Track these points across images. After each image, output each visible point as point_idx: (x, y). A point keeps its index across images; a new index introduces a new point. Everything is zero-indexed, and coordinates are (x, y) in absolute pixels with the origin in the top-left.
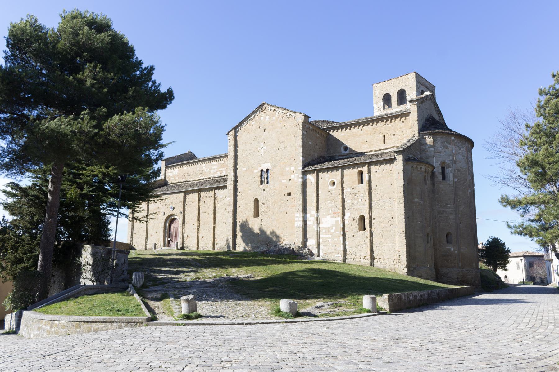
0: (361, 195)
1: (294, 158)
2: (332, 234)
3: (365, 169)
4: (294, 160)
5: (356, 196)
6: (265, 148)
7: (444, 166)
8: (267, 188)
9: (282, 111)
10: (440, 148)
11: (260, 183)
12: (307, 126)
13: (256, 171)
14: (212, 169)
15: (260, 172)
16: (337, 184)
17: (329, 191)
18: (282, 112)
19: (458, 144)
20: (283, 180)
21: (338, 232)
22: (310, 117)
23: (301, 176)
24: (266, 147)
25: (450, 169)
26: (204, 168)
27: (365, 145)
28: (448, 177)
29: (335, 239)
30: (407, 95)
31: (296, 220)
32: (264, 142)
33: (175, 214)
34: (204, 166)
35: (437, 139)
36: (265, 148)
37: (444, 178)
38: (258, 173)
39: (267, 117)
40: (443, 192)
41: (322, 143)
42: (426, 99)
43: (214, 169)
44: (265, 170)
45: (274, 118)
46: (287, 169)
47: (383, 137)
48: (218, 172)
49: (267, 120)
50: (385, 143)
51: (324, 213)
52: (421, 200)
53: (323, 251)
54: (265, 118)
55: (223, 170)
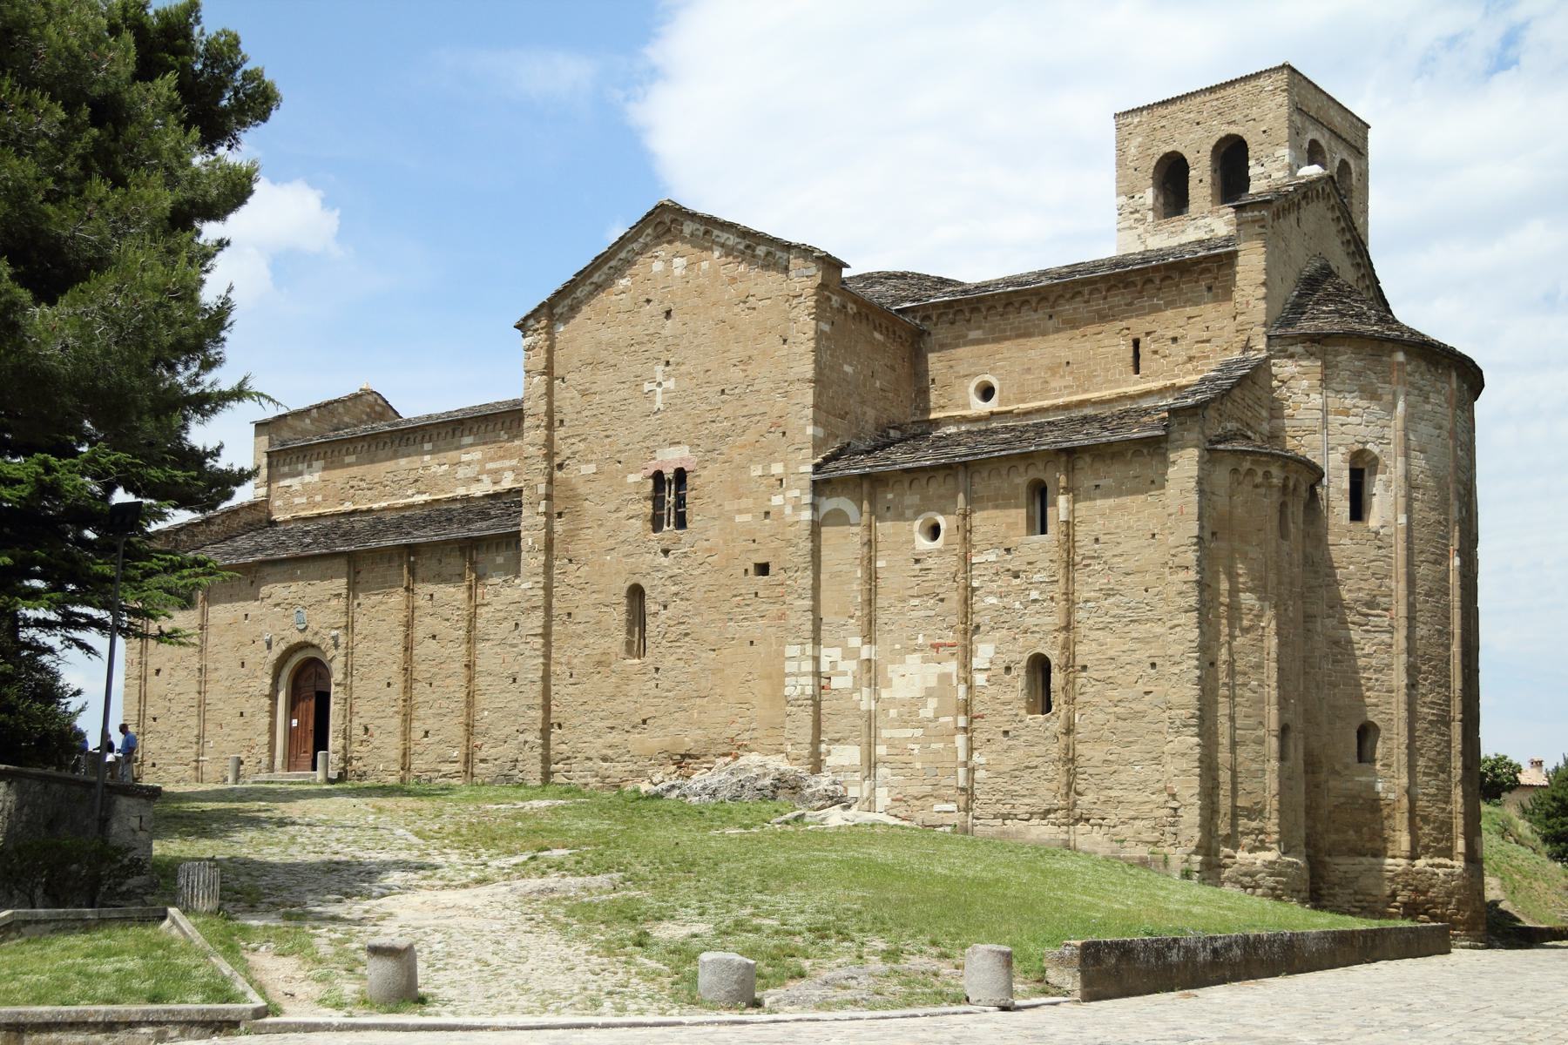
0: (1037, 577)
1: (781, 430)
4: (784, 433)
6: (670, 384)
7: (1360, 466)
8: (676, 546)
13: (632, 478)
15: (651, 481)
16: (948, 530)
20: (740, 512)
23: (807, 498)
24: (673, 379)
27: (1063, 377)
29: (934, 746)
30: (1251, 163)
32: (668, 363)
35: (1339, 359)
36: (670, 384)
37: (1358, 510)
41: (893, 368)
42: (1305, 196)
44: (669, 473)
45: (705, 265)
49: (677, 272)
50: (1137, 372)
55: (505, 469)
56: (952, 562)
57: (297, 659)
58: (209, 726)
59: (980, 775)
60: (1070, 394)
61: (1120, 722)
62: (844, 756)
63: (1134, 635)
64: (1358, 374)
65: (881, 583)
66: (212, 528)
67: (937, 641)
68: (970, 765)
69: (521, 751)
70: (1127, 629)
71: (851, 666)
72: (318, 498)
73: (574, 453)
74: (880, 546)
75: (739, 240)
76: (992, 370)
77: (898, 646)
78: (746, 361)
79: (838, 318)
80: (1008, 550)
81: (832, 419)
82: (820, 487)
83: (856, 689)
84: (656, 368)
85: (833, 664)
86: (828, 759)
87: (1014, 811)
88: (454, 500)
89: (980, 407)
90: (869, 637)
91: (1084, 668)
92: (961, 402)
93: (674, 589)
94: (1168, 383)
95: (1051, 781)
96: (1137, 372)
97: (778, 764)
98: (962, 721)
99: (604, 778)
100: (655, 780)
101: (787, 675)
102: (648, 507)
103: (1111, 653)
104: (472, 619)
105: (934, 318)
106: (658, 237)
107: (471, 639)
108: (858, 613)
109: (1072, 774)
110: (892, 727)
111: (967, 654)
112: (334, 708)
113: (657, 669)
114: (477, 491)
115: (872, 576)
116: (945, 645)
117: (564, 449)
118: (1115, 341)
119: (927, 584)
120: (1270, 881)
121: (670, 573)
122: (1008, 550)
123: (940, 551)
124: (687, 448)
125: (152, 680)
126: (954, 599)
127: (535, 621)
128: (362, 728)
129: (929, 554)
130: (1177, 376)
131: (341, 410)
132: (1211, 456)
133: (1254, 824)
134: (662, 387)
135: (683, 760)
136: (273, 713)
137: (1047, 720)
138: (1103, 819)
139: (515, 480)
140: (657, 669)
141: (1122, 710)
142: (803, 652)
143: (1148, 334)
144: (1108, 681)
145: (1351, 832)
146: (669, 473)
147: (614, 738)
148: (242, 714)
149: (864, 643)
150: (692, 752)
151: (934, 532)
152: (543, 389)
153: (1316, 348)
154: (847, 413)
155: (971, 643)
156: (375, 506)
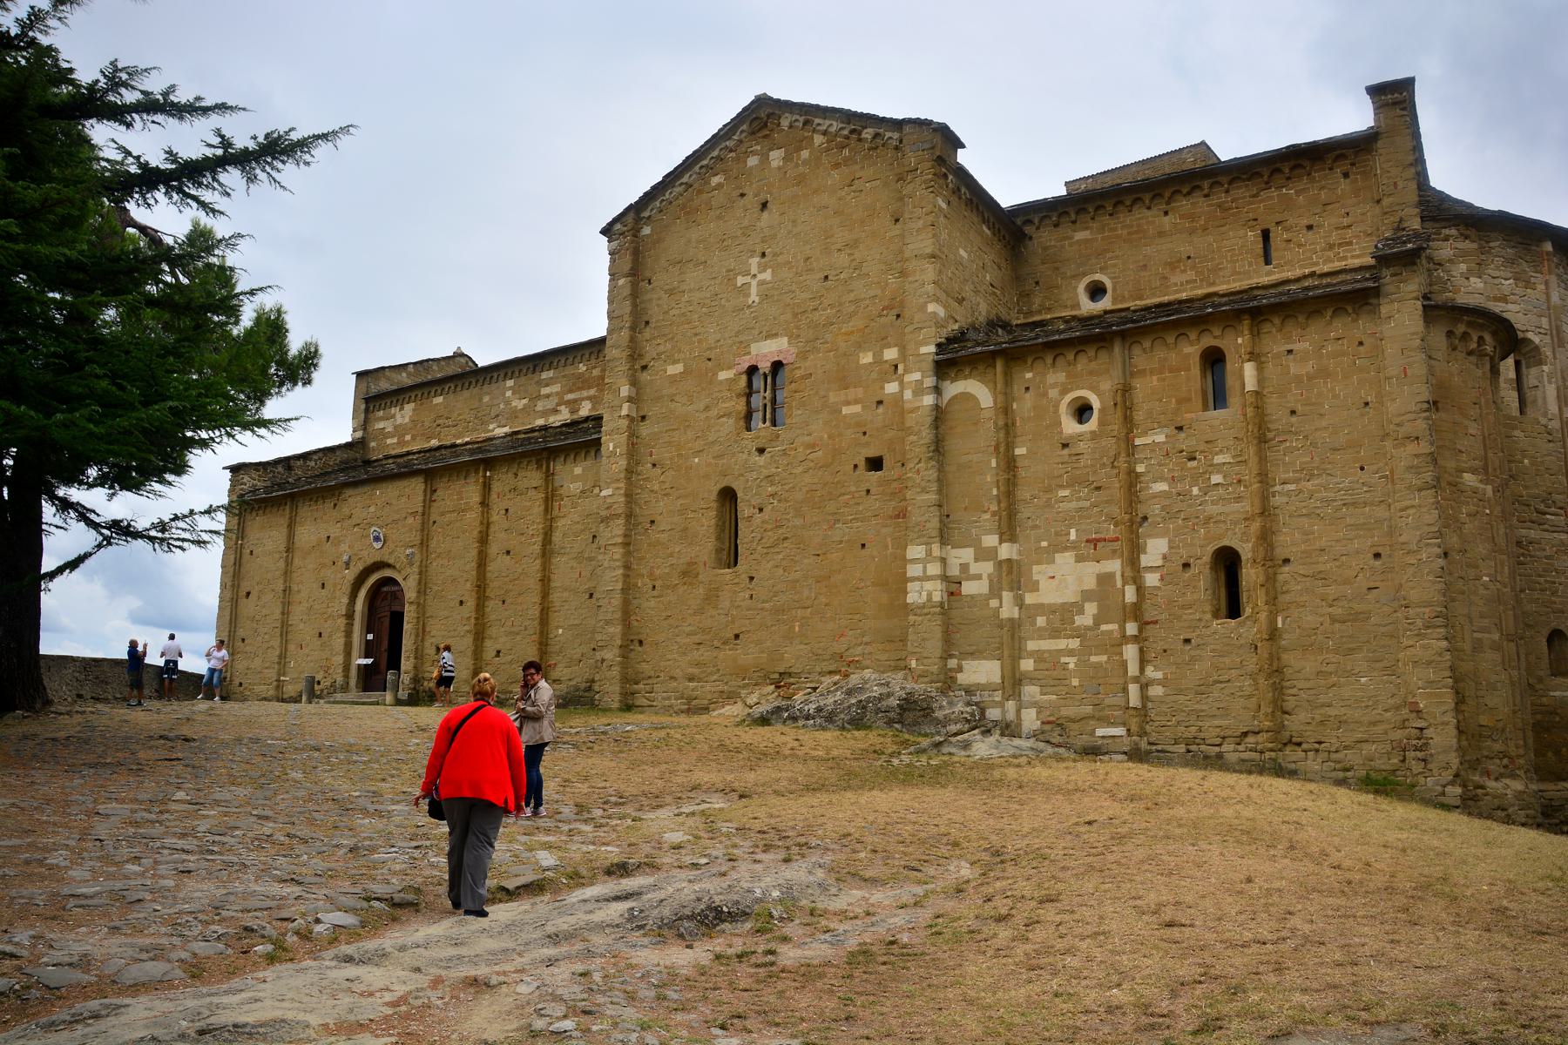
0: (1219, 459)
2: (1079, 633)
3: (1235, 343)
5: (1194, 463)
6: (767, 275)
8: (774, 444)
9: (841, 125)
10: (1503, 281)
11: (742, 423)
13: (723, 375)
14: (539, 397)
15: (744, 377)
16: (1102, 411)
18: (842, 129)
19: (1562, 270)
20: (848, 403)
21: (1113, 627)
22: (963, 146)
23: (930, 381)
24: (769, 271)
25: (1545, 368)
26: (509, 394)
27: (1184, 271)
28: (1534, 401)
29: (1094, 659)
31: (909, 574)
32: (763, 255)
33: (391, 561)
34: (510, 388)
35: (1492, 244)
36: (767, 275)
38: (730, 381)
39: (776, 157)
40: (1526, 461)
43: (548, 396)
44: (765, 366)
45: (805, 154)
46: (867, 358)
49: (775, 164)
50: (1268, 262)
51: (1044, 544)
52: (1486, 482)
53: (1038, 713)
54: (765, 158)
55: (583, 399)
56: (1109, 443)
58: (291, 647)
60: (1192, 289)
61: (1337, 625)
64: (1511, 262)
65: (1022, 473)
66: (308, 463)
68: (1143, 680)
70: (1338, 515)
71: (987, 568)
72: (408, 438)
75: (841, 125)
76: (1103, 270)
77: (1044, 544)
78: (854, 244)
79: (954, 199)
81: (951, 301)
84: (751, 261)
85: (964, 567)
86: (959, 675)
87: (1202, 735)
88: (532, 430)
89: (1088, 307)
90: (1009, 532)
91: (1287, 561)
92: (1069, 303)
94: (1307, 271)
95: (1250, 696)
96: (1268, 262)
98: (1131, 629)
99: (690, 700)
100: (749, 701)
102: (741, 406)
103: (1323, 543)
105: (1036, 221)
106: (753, 133)
108: (994, 507)
110: (1041, 638)
112: (406, 627)
113: (752, 578)
114: (555, 420)
116: (1105, 540)
117: (650, 350)
118: (1241, 233)
121: (766, 472)
122: (1180, 428)
123: (1092, 432)
124: (785, 339)
126: (1116, 488)
128: (434, 648)
130: (1317, 264)
131: (435, 368)
134: (756, 278)
136: (348, 633)
137: (1241, 625)
138: (1320, 743)
139: (593, 408)
140: (752, 578)
141: (1340, 611)
142: (929, 553)
145: (1550, 754)
147: (705, 654)
148: (320, 634)
150: (792, 670)
151: (1082, 411)
152: (627, 291)
153: (1472, 232)
154: (963, 299)
155: (1138, 537)
156: (458, 442)
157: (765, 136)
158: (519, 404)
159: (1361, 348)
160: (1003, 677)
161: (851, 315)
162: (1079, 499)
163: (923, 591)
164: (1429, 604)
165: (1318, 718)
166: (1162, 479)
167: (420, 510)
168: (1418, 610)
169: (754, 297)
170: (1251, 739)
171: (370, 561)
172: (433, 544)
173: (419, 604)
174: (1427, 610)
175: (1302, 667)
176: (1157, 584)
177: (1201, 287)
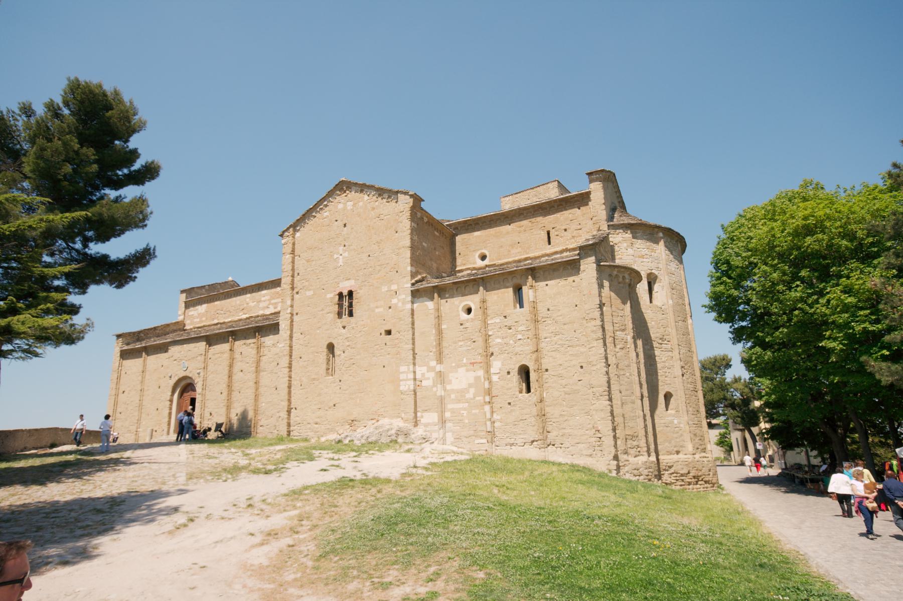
0: (520, 329)
1: (396, 270)
4: (397, 272)
5: (511, 331)
12: (419, 215)
15: (337, 297)
17: (461, 324)
20: (377, 307)
21: (481, 398)
22: (423, 201)
24: (347, 252)
29: (474, 411)
31: (401, 378)
32: (345, 246)
35: (638, 235)
36: (346, 254)
38: (332, 298)
43: (264, 301)
44: (345, 293)
45: (361, 204)
46: (385, 289)
47: (546, 235)
48: (271, 306)
49: (349, 208)
50: (549, 243)
53: (453, 434)
54: (345, 204)
55: (279, 302)
56: (478, 324)
57: (183, 383)
59: (497, 424)
60: (520, 255)
61: (567, 396)
62: (429, 418)
63: (570, 353)
67: (473, 361)
68: (492, 420)
69: (278, 421)
71: (432, 375)
72: (204, 319)
73: (303, 287)
74: (443, 319)
77: (454, 365)
80: (505, 317)
82: (416, 294)
83: (434, 386)
85: (423, 375)
86: (422, 419)
87: (516, 442)
89: (481, 263)
90: (440, 360)
91: (547, 370)
93: (347, 344)
94: (564, 248)
95: (534, 426)
97: (398, 423)
98: (487, 399)
100: (340, 433)
101: (401, 380)
102: (336, 308)
104: (258, 362)
107: (258, 370)
109: (544, 422)
111: (488, 367)
113: (340, 381)
114: (268, 312)
115: (440, 332)
116: (477, 363)
119: (466, 335)
120: (646, 472)
121: (346, 336)
122: (505, 317)
123: (472, 319)
125: (121, 396)
127: (285, 362)
129: (467, 321)
130: (568, 245)
132: (600, 269)
133: (635, 443)
134: (342, 256)
135: (352, 422)
137: (530, 396)
140: (340, 381)
141: (568, 389)
143: (553, 228)
144: (561, 376)
146: (345, 293)
148: (157, 409)
149: (437, 364)
150: (356, 419)
151: (469, 311)
152: (290, 260)
156: (226, 321)
157: (346, 196)
158: (252, 304)
159: (574, 283)
160: (438, 420)
161: (379, 271)
162: (467, 346)
163: (407, 385)
164: (601, 386)
165: (561, 434)
166: (498, 337)
167: (204, 353)
168: (597, 389)
169: (341, 263)
170: (535, 443)
171: (181, 376)
172: (209, 368)
173: (202, 394)
174: (600, 389)
175: (553, 412)
176: (498, 380)
177: (524, 255)
